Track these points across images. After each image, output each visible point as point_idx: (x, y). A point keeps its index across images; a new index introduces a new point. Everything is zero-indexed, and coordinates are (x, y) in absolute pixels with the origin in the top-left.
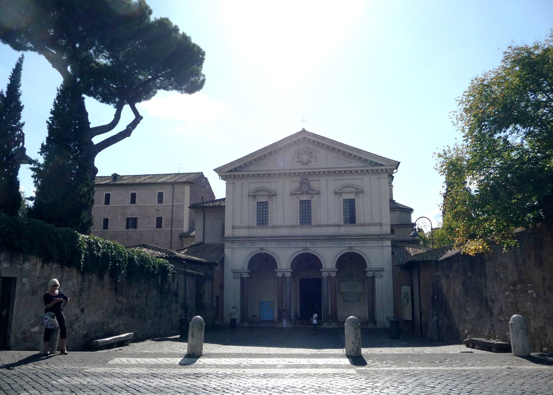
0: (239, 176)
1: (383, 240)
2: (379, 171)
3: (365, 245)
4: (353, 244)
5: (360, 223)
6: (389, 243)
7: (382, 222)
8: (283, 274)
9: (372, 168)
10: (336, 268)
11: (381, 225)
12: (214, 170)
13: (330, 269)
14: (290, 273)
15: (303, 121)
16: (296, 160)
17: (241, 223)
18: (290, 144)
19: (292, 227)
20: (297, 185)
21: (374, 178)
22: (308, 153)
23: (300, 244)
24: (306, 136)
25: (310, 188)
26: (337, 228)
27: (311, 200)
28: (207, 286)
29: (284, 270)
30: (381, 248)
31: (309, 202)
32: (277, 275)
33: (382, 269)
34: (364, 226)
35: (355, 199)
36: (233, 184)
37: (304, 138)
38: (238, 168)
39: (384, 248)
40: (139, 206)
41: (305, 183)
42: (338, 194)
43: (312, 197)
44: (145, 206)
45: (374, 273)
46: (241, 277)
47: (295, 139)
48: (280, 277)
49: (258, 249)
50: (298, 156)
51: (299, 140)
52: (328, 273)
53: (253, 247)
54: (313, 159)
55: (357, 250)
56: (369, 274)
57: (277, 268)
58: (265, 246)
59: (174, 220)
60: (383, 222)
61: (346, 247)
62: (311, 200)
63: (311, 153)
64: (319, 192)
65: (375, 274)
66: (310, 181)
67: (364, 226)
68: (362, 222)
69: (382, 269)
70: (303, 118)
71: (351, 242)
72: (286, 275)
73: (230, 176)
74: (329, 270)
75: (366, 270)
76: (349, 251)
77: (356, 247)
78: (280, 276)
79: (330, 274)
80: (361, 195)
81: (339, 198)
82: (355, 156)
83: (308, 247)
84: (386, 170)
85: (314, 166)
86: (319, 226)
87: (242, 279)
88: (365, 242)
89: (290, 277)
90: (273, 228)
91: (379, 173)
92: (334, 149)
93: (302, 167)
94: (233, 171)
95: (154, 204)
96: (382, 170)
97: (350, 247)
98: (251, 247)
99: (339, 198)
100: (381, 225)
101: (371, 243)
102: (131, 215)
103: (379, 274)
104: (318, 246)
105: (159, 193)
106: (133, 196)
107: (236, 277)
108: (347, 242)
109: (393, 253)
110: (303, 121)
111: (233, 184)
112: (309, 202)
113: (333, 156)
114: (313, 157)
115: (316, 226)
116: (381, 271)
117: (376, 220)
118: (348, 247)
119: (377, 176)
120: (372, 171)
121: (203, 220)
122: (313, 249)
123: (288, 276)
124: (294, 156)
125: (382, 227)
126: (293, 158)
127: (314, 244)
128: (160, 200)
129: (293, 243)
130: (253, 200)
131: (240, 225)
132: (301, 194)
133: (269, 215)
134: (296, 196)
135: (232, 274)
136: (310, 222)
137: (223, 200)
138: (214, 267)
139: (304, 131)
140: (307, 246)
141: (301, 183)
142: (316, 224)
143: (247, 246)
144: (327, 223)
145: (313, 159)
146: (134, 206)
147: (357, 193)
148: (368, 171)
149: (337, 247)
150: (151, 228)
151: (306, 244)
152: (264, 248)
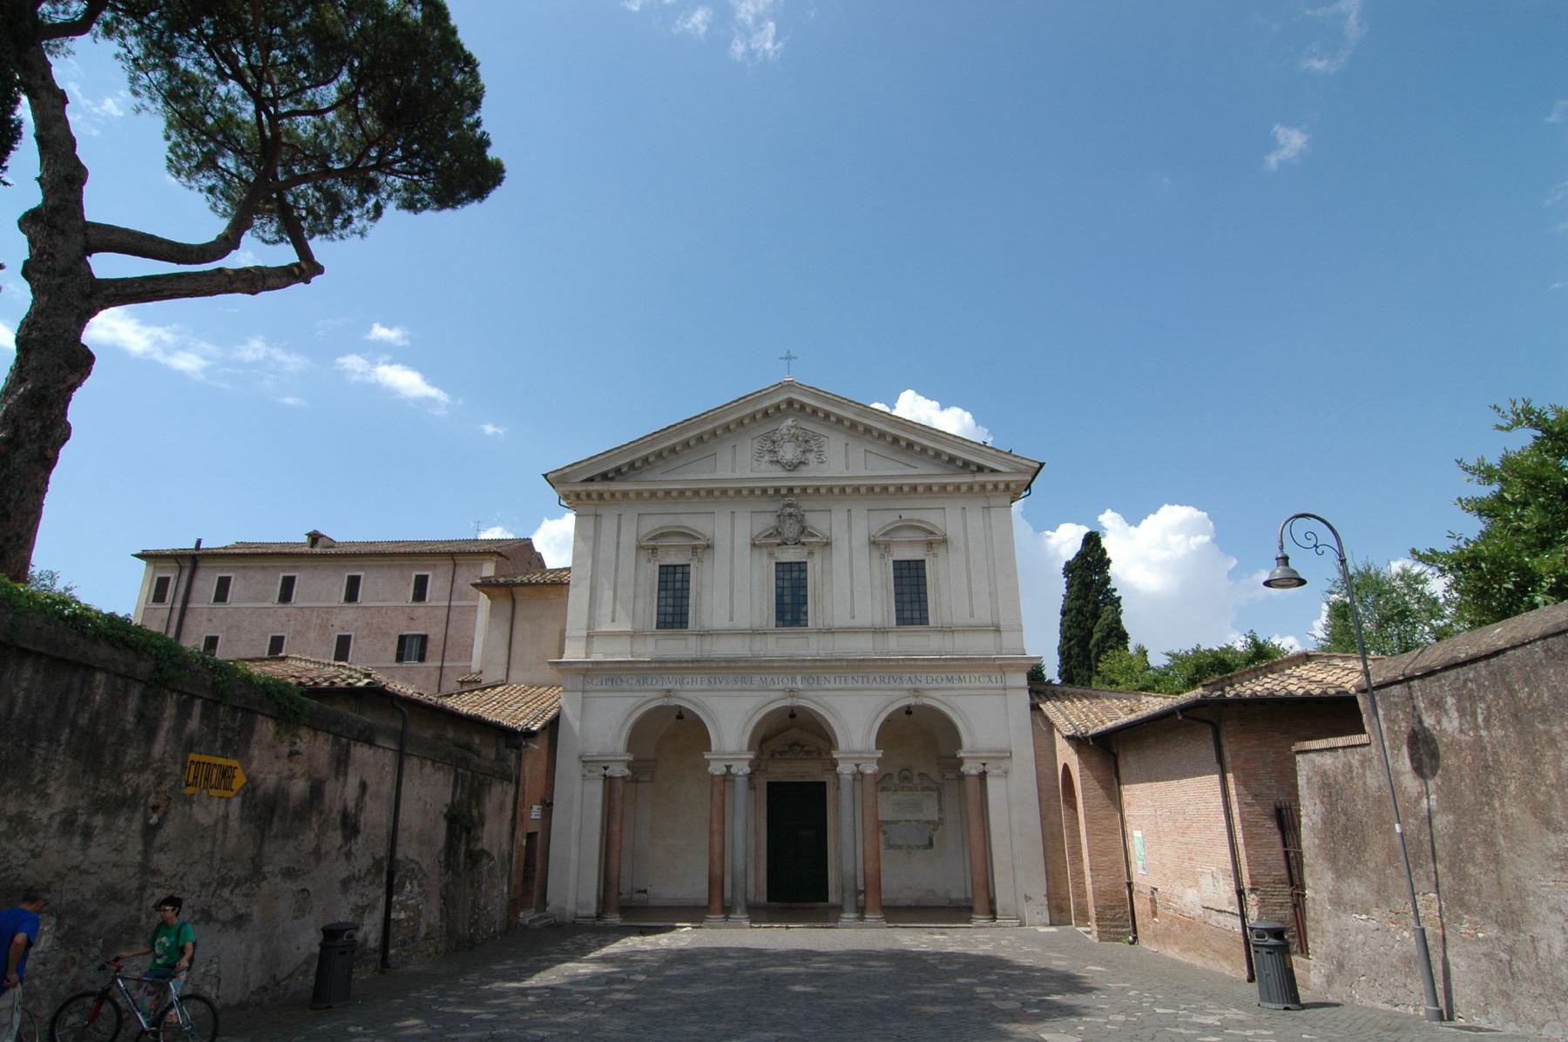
0: (613, 495)
2: (990, 487)
3: (957, 685)
4: (924, 682)
5: (939, 625)
8: (726, 766)
10: (877, 748)
12: (545, 476)
13: (860, 752)
14: (747, 763)
15: (789, 358)
19: (754, 633)
25: (803, 530)
27: (806, 563)
28: (498, 797)
29: (729, 754)
30: (1003, 692)
32: (709, 769)
33: (1005, 752)
34: (953, 631)
35: (923, 561)
36: (596, 516)
37: (790, 403)
39: (1008, 692)
41: (790, 515)
43: (811, 553)
47: (767, 403)
48: (717, 776)
51: (777, 408)
55: (935, 699)
56: (970, 768)
57: (710, 750)
58: (678, 687)
59: (449, 643)
61: (901, 690)
62: (806, 563)
63: (806, 441)
65: (987, 768)
67: (953, 631)
69: (1005, 752)
70: (788, 352)
71: (918, 675)
72: (733, 770)
73: (589, 495)
74: (857, 755)
78: (717, 773)
80: (941, 551)
81: (882, 557)
82: (924, 450)
84: (1007, 486)
85: (813, 472)
86: (830, 631)
88: (956, 676)
89: (745, 775)
92: (868, 430)
93: (785, 474)
95: (404, 604)
97: (916, 690)
99: (882, 557)
101: (973, 679)
104: (827, 686)
105: (417, 577)
106: (354, 583)
107: (589, 775)
108: (906, 677)
109: (1035, 708)
110: (789, 358)
111: (596, 516)
112: (801, 567)
114: (811, 451)
115: (820, 632)
116: (1002, 758)
117: (983, 616)
118: (909, 690)
120: (971, 487)
123: (740, 773)
128: (420, 593)
130: (649, 561)
132: (779, 545)
133: (691, 601)
134: (765, 551)
137: (568, 569)
140: (794, 685)
143: (625, 685)
144: (851, 623)
145: (811, 457)
147: (930, 544)
148: (958, 487)
149: (879, 689)
151: (794, 680)
152: (675, 690)
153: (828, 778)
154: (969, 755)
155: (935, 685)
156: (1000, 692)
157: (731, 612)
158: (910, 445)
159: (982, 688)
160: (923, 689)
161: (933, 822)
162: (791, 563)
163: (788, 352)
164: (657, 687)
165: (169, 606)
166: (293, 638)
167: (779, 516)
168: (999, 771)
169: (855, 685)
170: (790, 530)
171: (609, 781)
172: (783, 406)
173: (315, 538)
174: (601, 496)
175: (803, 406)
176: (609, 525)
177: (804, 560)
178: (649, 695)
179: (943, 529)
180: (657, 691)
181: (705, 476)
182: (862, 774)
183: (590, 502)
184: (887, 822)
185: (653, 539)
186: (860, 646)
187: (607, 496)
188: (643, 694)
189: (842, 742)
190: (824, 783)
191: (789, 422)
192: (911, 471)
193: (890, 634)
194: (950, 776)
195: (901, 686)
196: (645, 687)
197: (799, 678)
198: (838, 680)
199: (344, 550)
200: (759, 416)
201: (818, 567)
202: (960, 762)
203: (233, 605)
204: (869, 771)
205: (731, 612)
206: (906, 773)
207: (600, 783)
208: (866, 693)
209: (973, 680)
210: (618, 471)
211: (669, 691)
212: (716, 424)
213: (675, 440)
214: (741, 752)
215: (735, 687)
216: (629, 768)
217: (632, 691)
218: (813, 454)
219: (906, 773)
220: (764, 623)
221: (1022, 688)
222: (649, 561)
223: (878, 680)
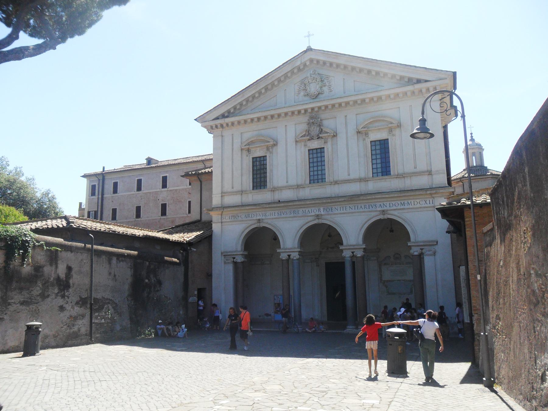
3: (406, 207)
4: (388, 206)
7: (431, 169)
12: (196, 120)
13: (354, 246)
14: (297, 253)
17: (233, 188)
18: (292, 72)
20: (304, 127)
22: (318, 80)
23: (310, 211)
24: (313, 57)
26: (363, 184)
27: (324, 148)
31: (322, 150)
34: (404, 177)
37: (311, 61)
40: (171, 190)
41: (313, 123)
42: (362, 133)
44: (176, 190)
45: (422, 249)
46: (234, 261)
47: (298, 63)
50: (304, 88)
53: (247, 219)
54: (325, 89)
57: (280, 248)
58: (264, 217)
60: (433, 170)
61: (376, 211)
62: (324, 148)
64: (335, 134)
65: (423, 251)
68: (401, 172)
71: (385, 203)
72: (291, 257)
74: (352, 247)
76: (382, 217)
77: (392, 210)
78: (284, 259)
79: (354, 253)
80: (397, 132)
83: (322, 215)
86: (336, 183)
88: (406, 202)
89: (297, 259)
92: (353, 69)
95: (186, 187)
97: (383, 211)
98: (245, 219)
100: (430, 173)
102: (163, 201)
103: (429, 251)
104: (336, 212)
107: (227, 261)
108: (378, 204)
111: (222, 136)
112: (321, 150)
114: (325, 86)
115: (331, 183)
117: (422, 166)
118: (380, 211)
120: (413, 93)
121: (200, 191)
122: (328, 217)
123: (295, 258)
124: (300, 88)
125: (432, 177)
129: (301, 210)
130: (247, 156)
131: (230, 190)
133: (268, 174)
134: (303, 143)
136: (323, 180)
138: (189, 248)
139: (309, 49)
140: (319, 213)
142: (332, 181)
143: (240, 218)
146: (165, 191)
148: (405, 94)
149: (364, 212)
150: (183, 214)
151: (319, 210)
154: (413, 244)
155: (394, 208)
157: (287, 178)
159: (420, 208)
160: (387, 210)
165: (97, 197)
166: (144, 206)
169: (351, 211)
171: (235, 263)
173: (149, 161)
174: (222, 126)
175: (318, 61)
183: (218, 130)
184: (388, 281)
187: (225, 125)
189: (345, 242)
193: (369, 181)
195: (375, 209)
196: (249, 218)
197: (322, 209)
198: (342, 209)
199: (163, 164)
200: (296, 71)
201: (330, 150)
203: (120, 194)
204: (359, 255)
205: (287, 178)
209: (416, 203)
210: (229, 112)
211: (259, 220)
212: (274, 79)
213: (254, 92)
214: (295, 248)
215: (291, 216)
217: (243, 221)
218: (326, 87)
222: (247, 156)
223: (363, 207)
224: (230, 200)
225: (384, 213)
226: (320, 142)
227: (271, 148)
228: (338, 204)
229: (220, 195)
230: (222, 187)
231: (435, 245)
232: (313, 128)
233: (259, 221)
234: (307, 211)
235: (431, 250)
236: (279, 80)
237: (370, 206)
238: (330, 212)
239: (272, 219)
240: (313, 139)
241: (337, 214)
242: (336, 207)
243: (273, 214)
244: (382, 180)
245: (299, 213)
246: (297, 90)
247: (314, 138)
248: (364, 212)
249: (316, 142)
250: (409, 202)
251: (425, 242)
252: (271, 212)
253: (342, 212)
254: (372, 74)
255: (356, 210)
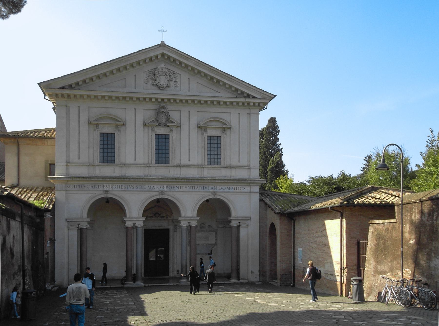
0: (75, 96)
1: (250, 186)
2: (252, 104)
3: (231, 191)
4: (218, 189)
5: (226, 165)
6: (257, 189)
7: (250, 164)
8: (133, 223)
9: (243, 100)
11: (249, 168)
14: (142, 222)
15: (163, 31)
16: (151, 82)
21: (244, 112)
22: (167, 74)
24: (165, 52)
27: (169, 135)
30: (249, 194)
33: (248, 218)
34: (231, 168)
37: (163, 55)
38: (73, 86)
43: (171, 131)
45: (239, 222)
47: (152, 54)
49: (101, 192)
51: (157, 57)
52: (188, 223)
54: (172, 83)
55: (222, 196)
56: (234, 224)
57: (125, 216)
58: (111, 189)
60: (251, 165)
61: (209, 192)
62: (169, 135)
63: (170, 76)
65: (240, 224)
66: (168, 110)
70: (162, 27)
71: (215, 186)
73: (63, 95)
74: (189, 219)
75: (231, 219)
76: (213, 197)
78: (129, 226)
80: (228, 132)
82: (225, 84)
83: (165, 191)
84: (259, 104)
86: (179, 166)
87: (81, 231)
88: (231, 187)
90: (122, 166)
91: (250, 107)
92: (199, 72)
93: (159, 92)
94: (67, 89)
96: (254, 104)
97: (215, 192)
99: (203, 134)
104: (177, 190)
107: (71, 227)
108: (210, 187)
109: (261, 200)
112: (167, 137)
113: (197, 82)
114: (172, 81)
117: (244, 162)
118: (212, 192)
119: (247, 111)
120: (243, 103)
122: (171, 193)
123: (140, 226)
126: (147, 80)
127: (172, 188)
132: (157, 126)
135: (66, 224)
136: (167, 162)
141: (158, 112)
142: (175, 164)
143: (86, 188)
145: (172, 83)
147: (224, 129)
148: (238, 103)
149: (199, 192)
151: (163, 187)
152: (110, 191)
153: (171, 228)
155: (222, 190)
156: (248, 194)
158: (218, 81)
159: (241, 192)
160: (217, 192)
161: (213, 244)
162: (162, 135)
163: (162, 27)
164: (101, 189)
167: (157, 112)
168: (245, 225)
170: (163, 119)
172: (159, 57)
174: (69, 96)
175: (169, 57)
176: (73, 111)
177: (168, 134)
178: (98, 193)
179: (229, 122)
180: (100, 191)
181: (121, 90)
182: (191, 226)
185: (96, 120)
186: (193, 173)
187: (72, 96)
188: (94, 192)
189: (183, 214)
190: (169, 229)
191: (163, 65)
192: (217, 95)
193: (204, 168)
194: (221, 226)
195: (208, 191)
196: (96, 189)
197: (165, 186)
200: (148, 61)
202: (230, 221)
206: (203, 225)
207: (77, 230)
208: (193, 193)
209: (238, 188)
210: (77, 84)
212: (127, 63)
213: (106, 70)
216: (88, 223)
217: (89, 191)
219: (203, 225)
220: (150, 162)
221: (257, 192)
222: (95, 130)
223: (199, 188)
224: (75, 171)
225: (215, 194)
226: (166, 129)
227: (120, 127)
228: (180, 183)
229: (65, 164)
230: (68, 156)
231: (249, 220)
232: (161, 117)
233: (107, 192)
234: (152, 187)
235: (246, 224)
236: (132, 65)
237: (204, 187)
238: (172, 190)
239: (120, 191)
240: (160, 126)
241: (178, 192)
242: (177, 186)
243: (120, 187)
244: (215, 169)
245: (145, 188)
246: (146, 78)
247: (161, 125)
248: (199, 192)
249: (162, 129)
250: (233, 188)
251: (243, 217)
252: (118, 185)
253: (182, 190)
254: (214, 81)
255: (194, 190)
